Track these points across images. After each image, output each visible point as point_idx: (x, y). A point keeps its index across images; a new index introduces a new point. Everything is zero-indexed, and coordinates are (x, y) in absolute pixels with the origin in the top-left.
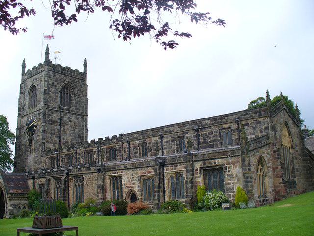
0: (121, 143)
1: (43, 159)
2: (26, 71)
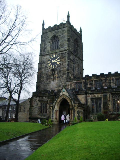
1: (68, 83)
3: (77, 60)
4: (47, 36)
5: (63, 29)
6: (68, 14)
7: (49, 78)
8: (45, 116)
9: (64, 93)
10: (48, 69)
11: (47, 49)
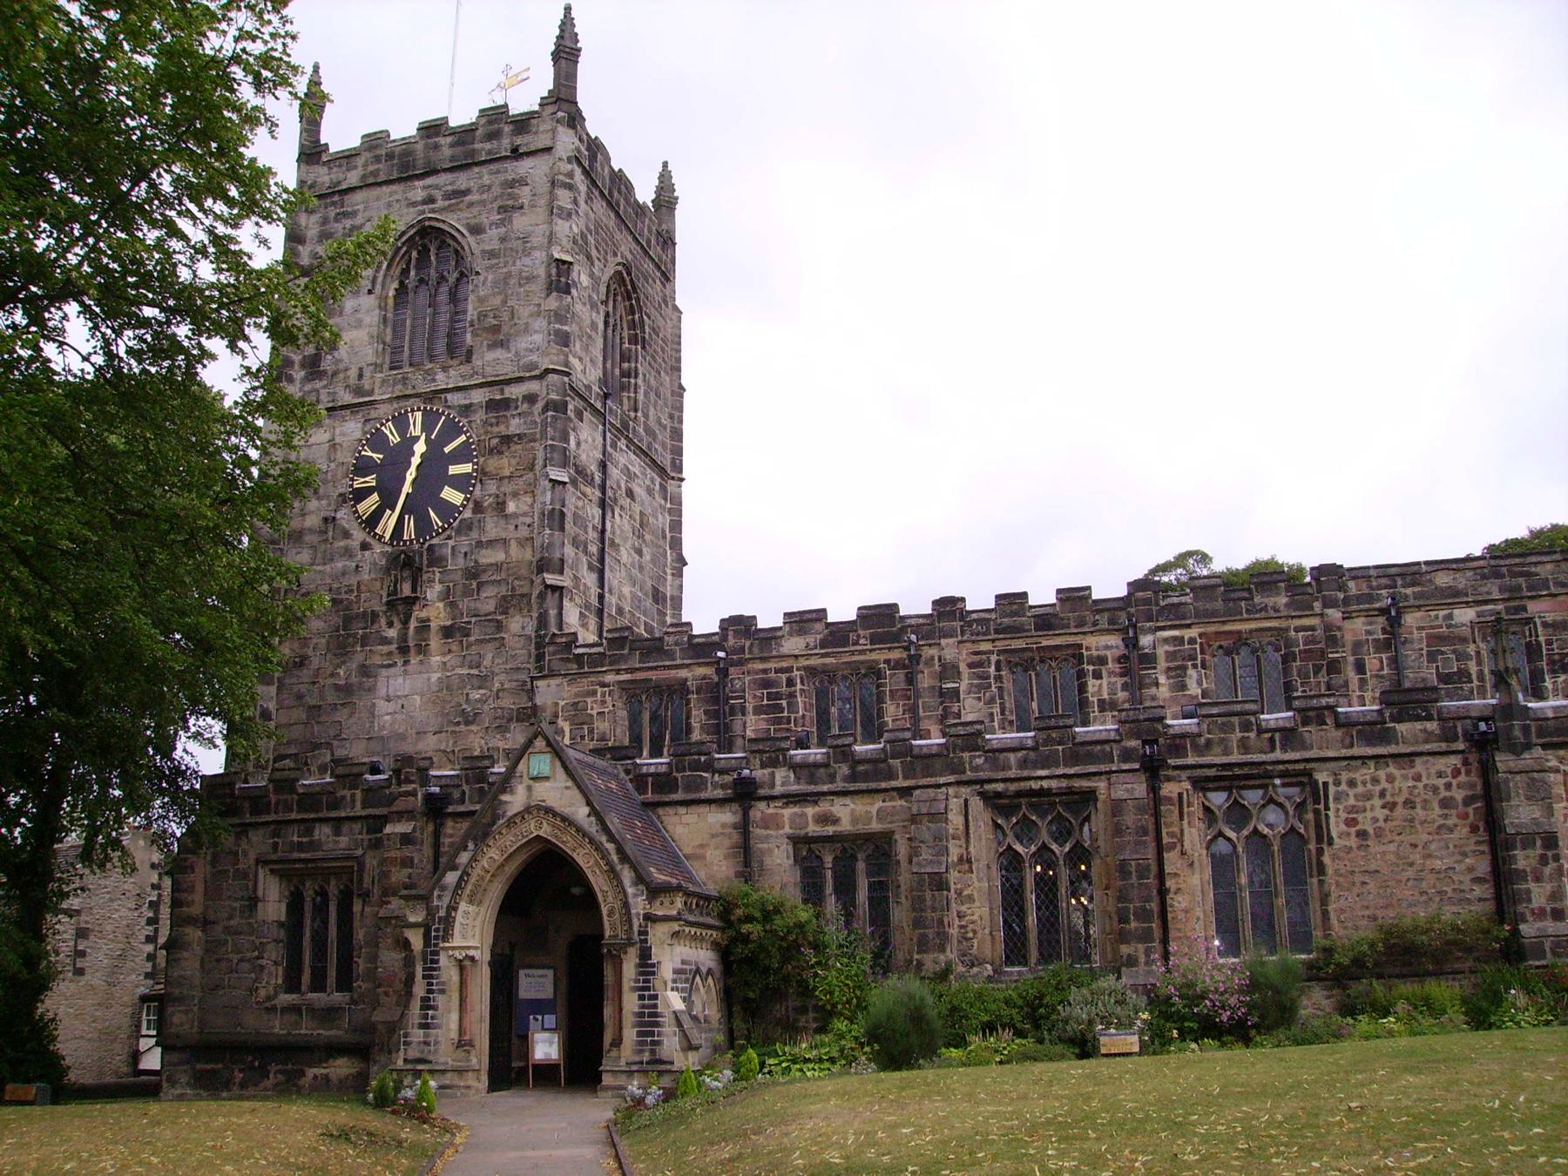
0: (1334, 614)
1: (550, 693)
2: (339, 134)
4: (348, 223)
5: (508, 165)
6: (567, 23)
7: (365, 641)
8: (329, 1015)
9: (545, 790)
10: (348, 553)
11: (343, 352)
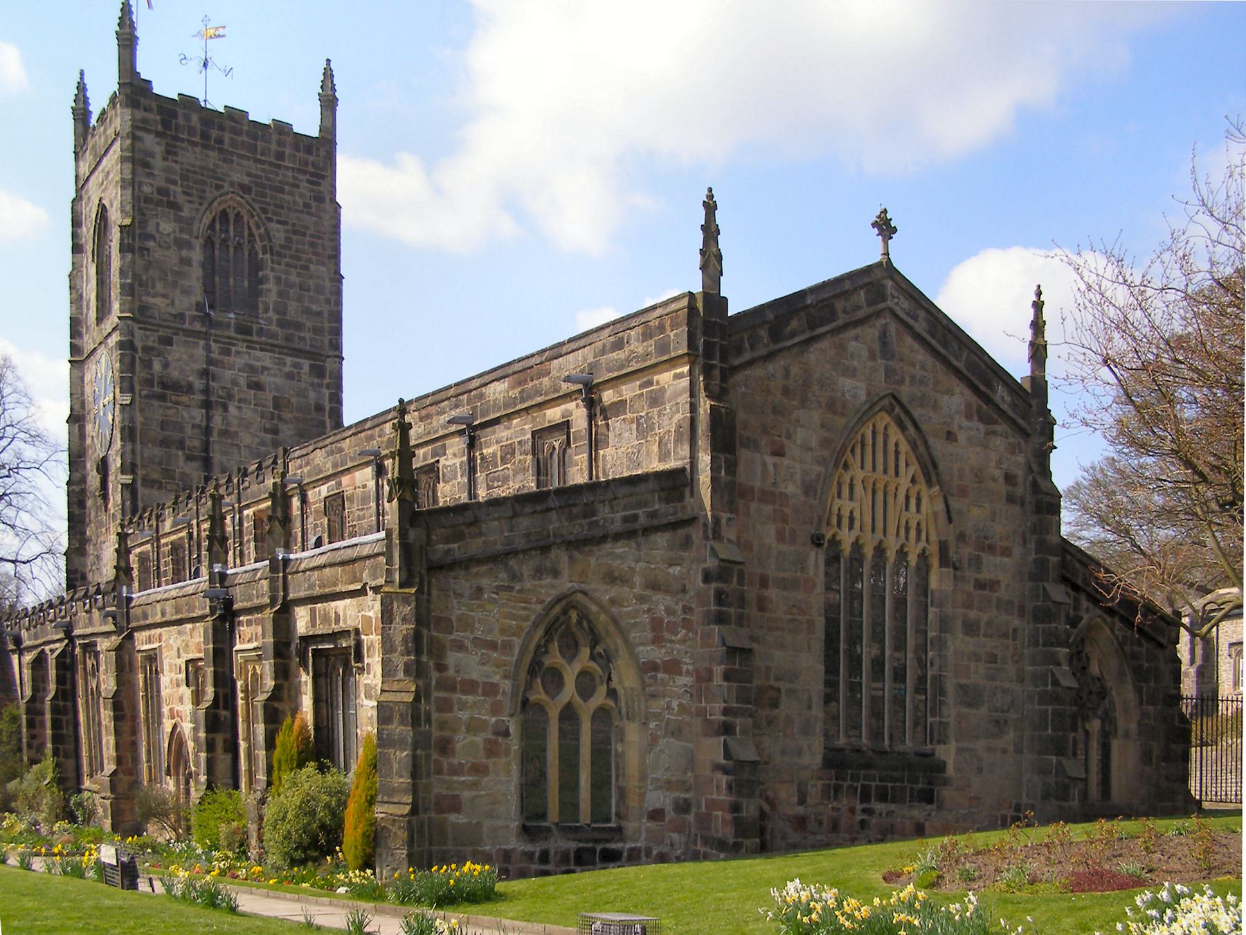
3: (251, 369)
